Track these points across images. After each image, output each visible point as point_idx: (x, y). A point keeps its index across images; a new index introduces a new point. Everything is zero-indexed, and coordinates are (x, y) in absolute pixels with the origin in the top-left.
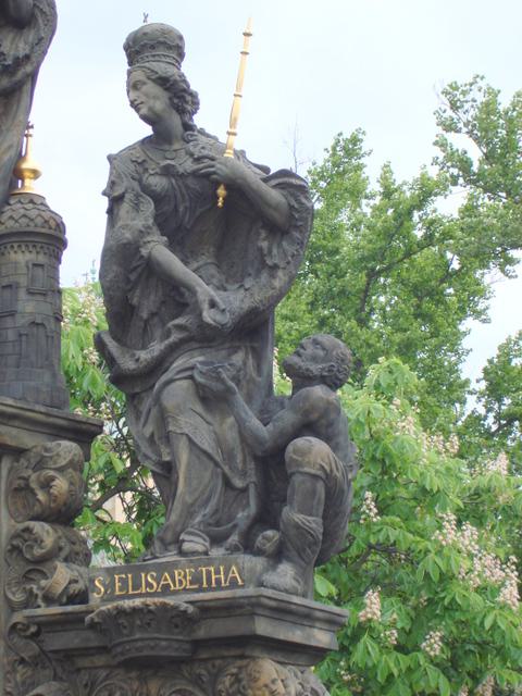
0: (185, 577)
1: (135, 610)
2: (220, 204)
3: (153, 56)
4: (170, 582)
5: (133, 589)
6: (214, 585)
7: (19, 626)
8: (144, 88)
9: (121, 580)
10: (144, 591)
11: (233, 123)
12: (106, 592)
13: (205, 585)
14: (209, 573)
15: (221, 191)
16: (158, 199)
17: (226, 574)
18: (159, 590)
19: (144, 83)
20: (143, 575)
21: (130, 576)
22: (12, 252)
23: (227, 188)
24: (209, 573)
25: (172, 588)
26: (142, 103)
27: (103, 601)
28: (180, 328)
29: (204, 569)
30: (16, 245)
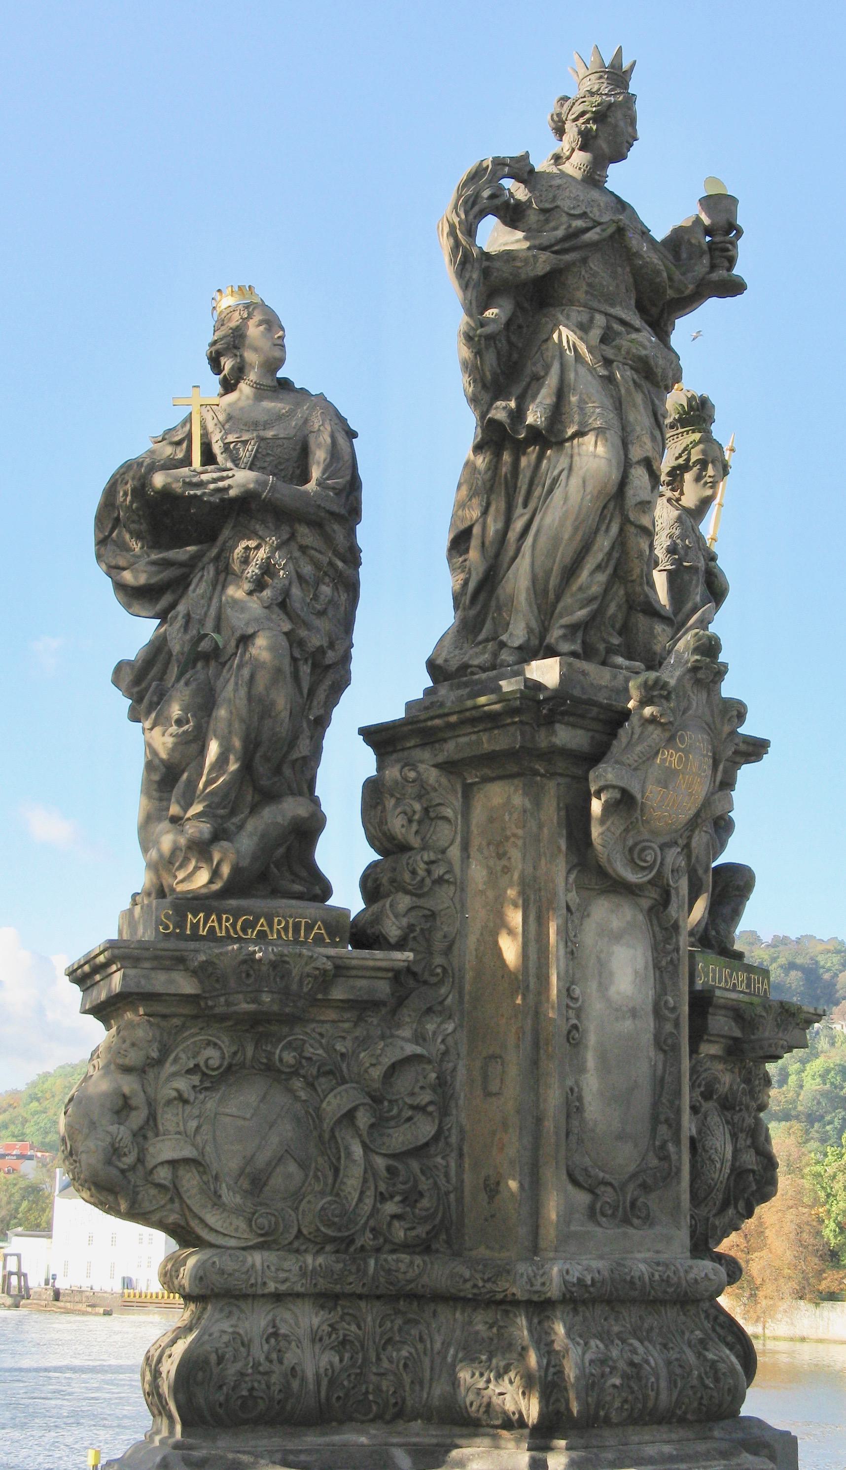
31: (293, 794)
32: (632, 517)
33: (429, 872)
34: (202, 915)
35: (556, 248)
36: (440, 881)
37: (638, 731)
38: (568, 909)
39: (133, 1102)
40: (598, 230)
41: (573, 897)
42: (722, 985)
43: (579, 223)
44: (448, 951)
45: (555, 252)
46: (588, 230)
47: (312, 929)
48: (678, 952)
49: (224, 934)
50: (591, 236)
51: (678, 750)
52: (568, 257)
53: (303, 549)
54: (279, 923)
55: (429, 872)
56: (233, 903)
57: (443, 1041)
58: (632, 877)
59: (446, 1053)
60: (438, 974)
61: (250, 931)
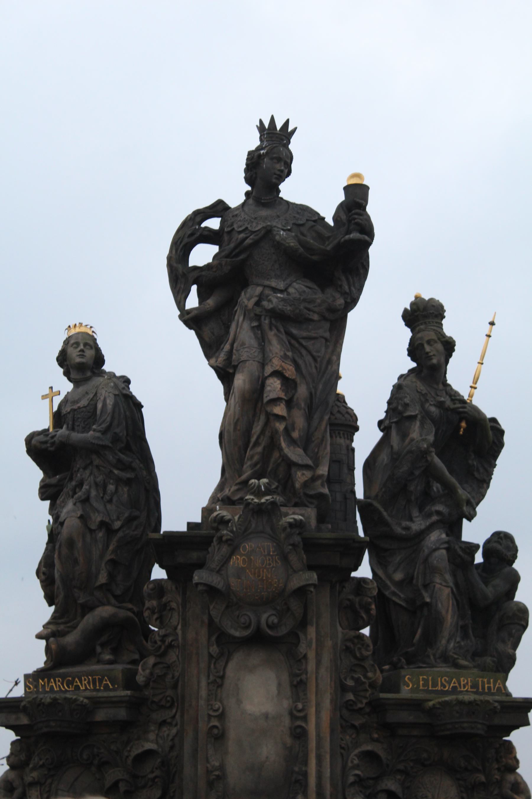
0: (467, 683)
1: (470, 703)
2: (461, 433)
3: (424, 317)
4: (457, 685)
5: (432, 687)
6: (486, 690)
7: (352, 703)
8: (435, 345)
9: (423, 679)
10: (439, 689)
11: (476, 381)
12: (413, 686)
13: (480, 690)
14: (483, 683)
15: (463, 424)
16: (433, 421)
17: (494, 686)
18: (450, 690)
19: (436, 342)
20: (439, 679)
21: (430, 678)
22: (338, 438)
23: (467, 423)
24: (483, 683)
25: (459, 689)
26: (434, 355)
27: (412, 690)
28: (438, 513)
29: (480, 680)
30: (341, 433)
31: (104, 604)
32: (269, 409)
33: (163, 641)
34: (46, 680)
35: (234, 253)
36: (171, 646)
37: (217, 548)
38: (211, 656)
39: (15, 785)
40: (251, 237)
41: (214, 650)
42: (439, 688)
43: (242, 235)
44: (175, 687)
45: (233, 257)
46: (246, 238)
47: (102, 682)
48: (306, 674)
49: (58, 689)
50: (248, 241)
51: (241, 555)
52: (242, 257)
53: (97, 467)
54: (85, 680)
55: (163, 641)
56: (62, 671)
57: (172, 740)
58: (237, 634)
59: (172, 747)
60: (169, 701)
61: (71, 687)
